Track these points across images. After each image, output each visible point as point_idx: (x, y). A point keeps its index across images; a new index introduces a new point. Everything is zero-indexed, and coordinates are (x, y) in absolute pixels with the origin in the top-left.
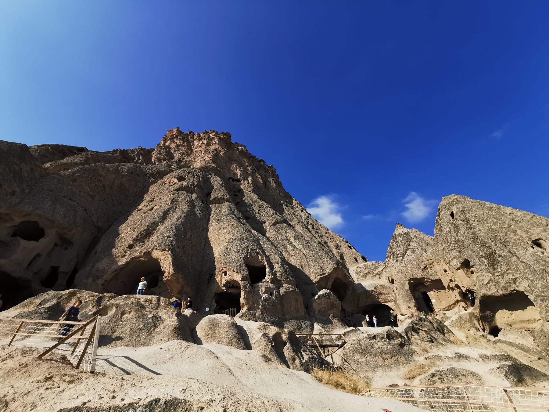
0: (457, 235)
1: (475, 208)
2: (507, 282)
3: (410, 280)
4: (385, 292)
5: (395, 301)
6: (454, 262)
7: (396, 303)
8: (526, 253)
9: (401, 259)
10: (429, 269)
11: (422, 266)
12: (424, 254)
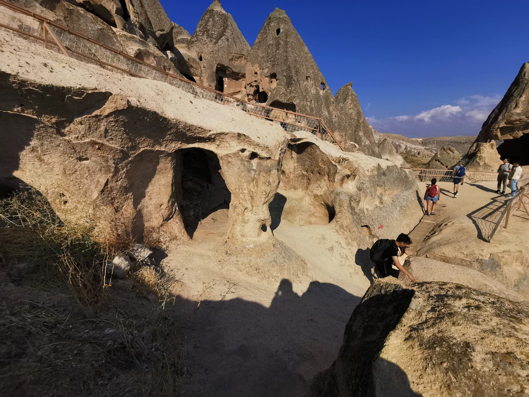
0: (276, 51)
1: (295, 38)
2: (291, 97)
3: (218, 64)
4: (194, 66)
5: (200, 77)
6: (266, 71)
7: (200, 78)
8: (303, 83)
9: (214, 41)
10: (233, 61)
11: (230, 57)
12: (234, 47)
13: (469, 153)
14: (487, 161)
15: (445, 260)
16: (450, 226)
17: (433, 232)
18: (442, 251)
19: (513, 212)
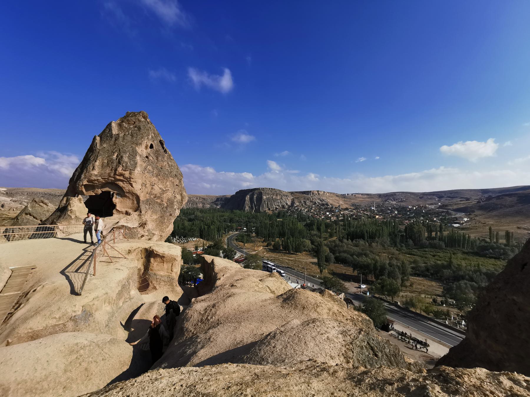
13: (60, 207)
14: (78, 214)
15: (34, 336)
16: (39, 291)
17: (18, 305)
18: (28, 327)
19: (98, 259)
